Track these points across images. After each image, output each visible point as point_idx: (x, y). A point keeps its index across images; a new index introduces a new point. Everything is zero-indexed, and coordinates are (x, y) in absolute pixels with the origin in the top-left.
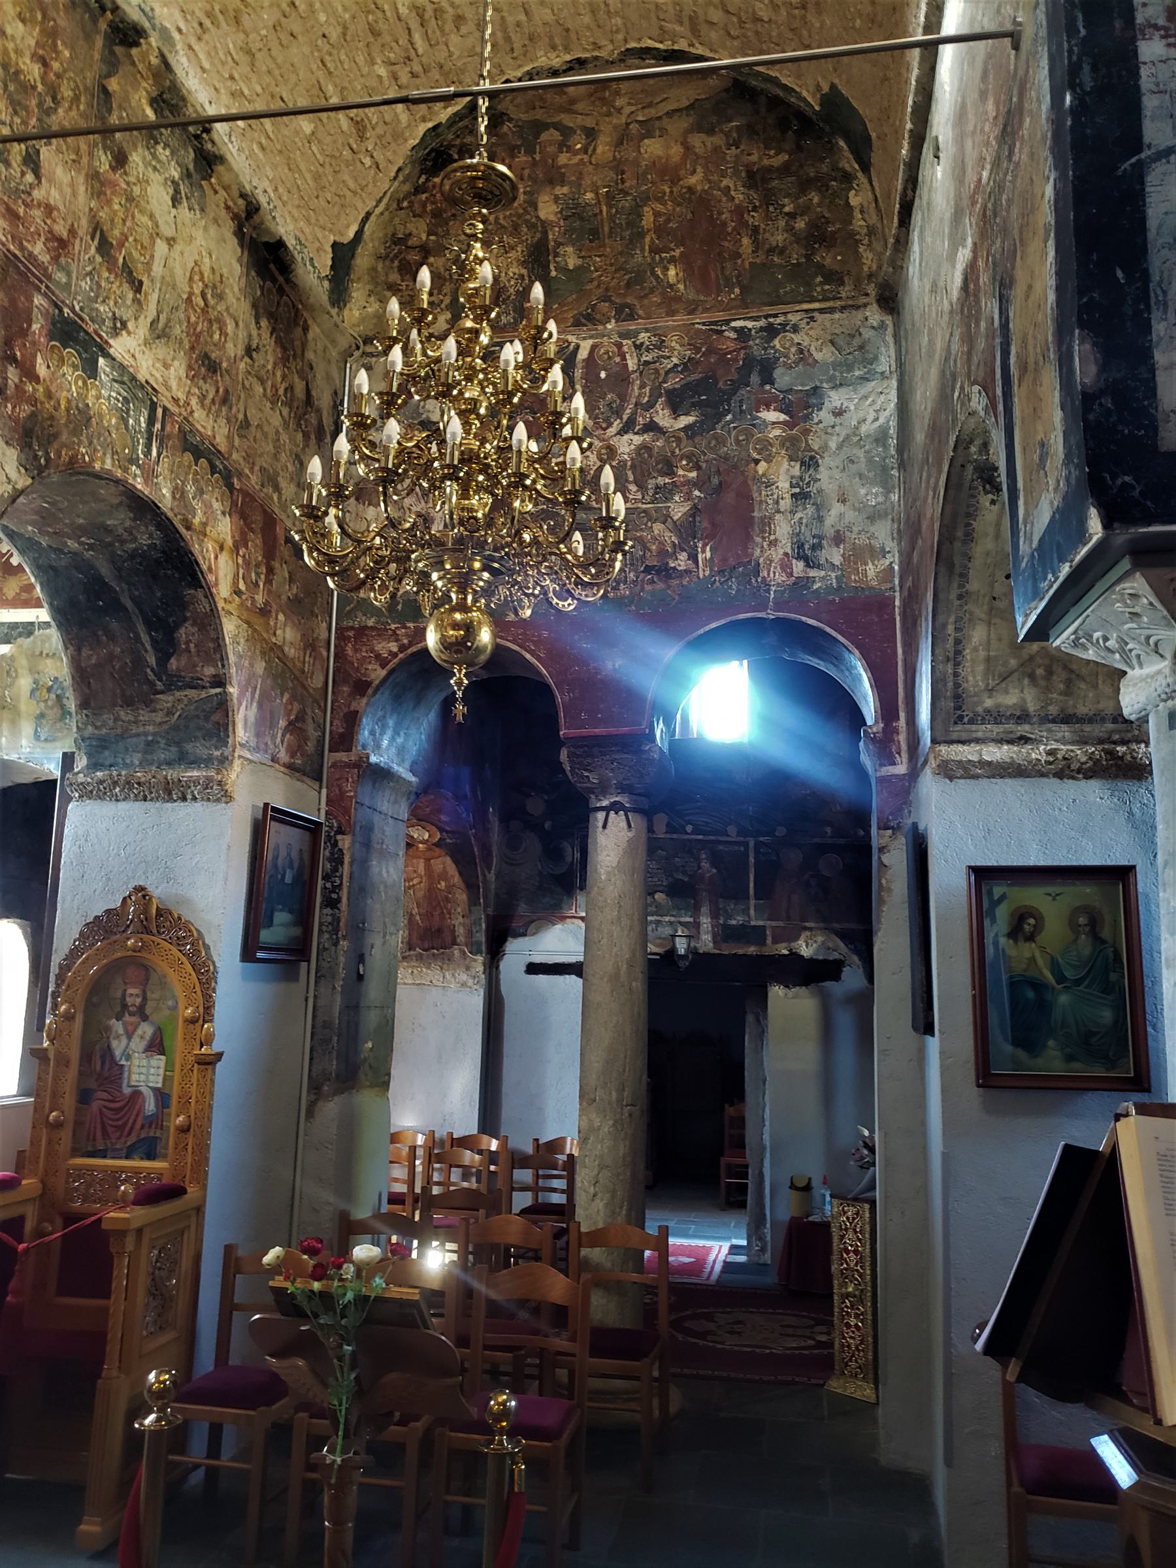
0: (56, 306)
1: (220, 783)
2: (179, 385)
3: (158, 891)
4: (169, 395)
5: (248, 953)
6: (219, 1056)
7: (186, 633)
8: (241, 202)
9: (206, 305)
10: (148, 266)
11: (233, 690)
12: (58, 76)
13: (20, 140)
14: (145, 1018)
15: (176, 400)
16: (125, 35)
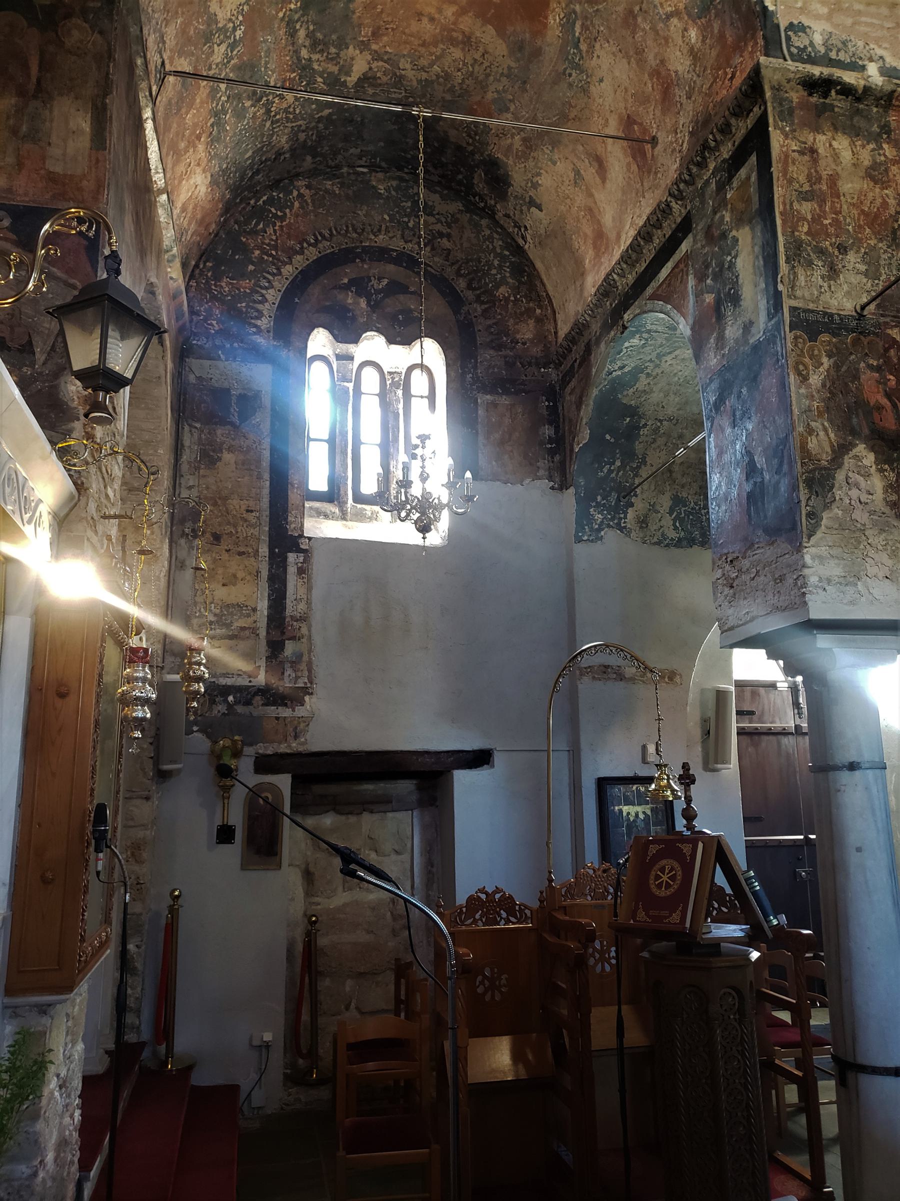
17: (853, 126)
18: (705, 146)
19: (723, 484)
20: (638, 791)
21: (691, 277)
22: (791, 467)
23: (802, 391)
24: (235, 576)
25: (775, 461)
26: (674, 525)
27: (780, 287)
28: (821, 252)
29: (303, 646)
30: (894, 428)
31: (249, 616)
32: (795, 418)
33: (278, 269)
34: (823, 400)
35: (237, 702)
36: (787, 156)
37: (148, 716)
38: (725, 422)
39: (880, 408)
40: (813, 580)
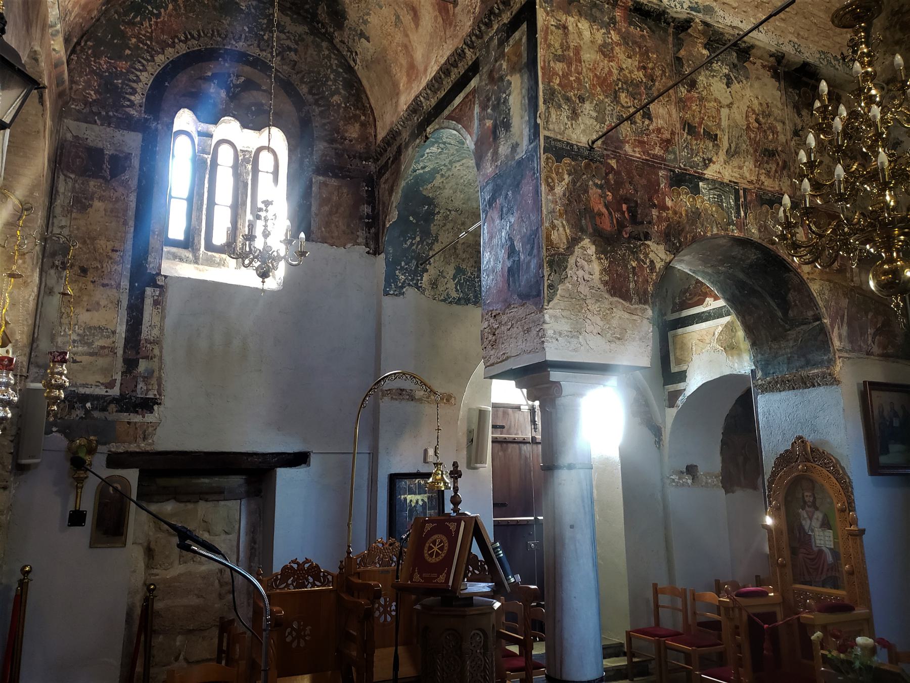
0: (671, 171)
1: (830, 374)
2: (751, 174)
3: (810, 438)
4: (745, 181)
5: (875, 468)
6: (863, 532)
7: (791, 296)
8: (772, 59)
9: (760, 124)
10: (719, 125)
11: (826, 321)
12: (652, 69)
13: (638, 111)
14: (817, 509)
15: (751, 182)
16: (682, 27)
17: (592, 15)
18: (491, 12)
19: (492, 261)
21: (477, 106)
22: (539, 251)
23: (550, 197)
24: (98, 303)
25: (528, 247)
26: (456, 288)
27: (539, 121)
28: (568, 99)
29: (155, 364)
30: (609, 229)
31: (108, 337)
32: (544, 216)
33: (152, 56)
34: (563, 205)
35: (94, 408)
36: (547, 28)
37: (9, 415)
38: (495, 215)
39: (600, 214)
40: (550, 332)
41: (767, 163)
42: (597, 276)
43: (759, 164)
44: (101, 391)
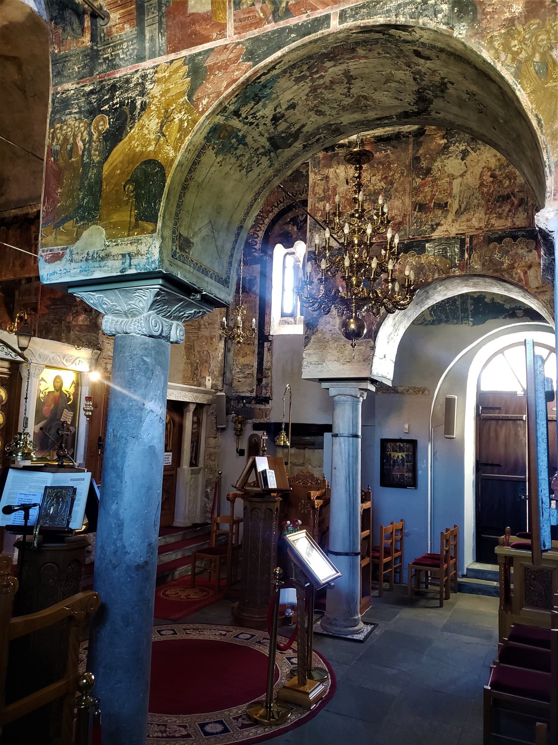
16: (419, 133)
20: (400, 445)
24: (246, 353)
26: (430, 313)
31: (251, 369)
33: (263, 221)
35: (246, 403)
41: (500, 207)
42: (337, 327)
43: (489, 211)
44: (248, 394)
